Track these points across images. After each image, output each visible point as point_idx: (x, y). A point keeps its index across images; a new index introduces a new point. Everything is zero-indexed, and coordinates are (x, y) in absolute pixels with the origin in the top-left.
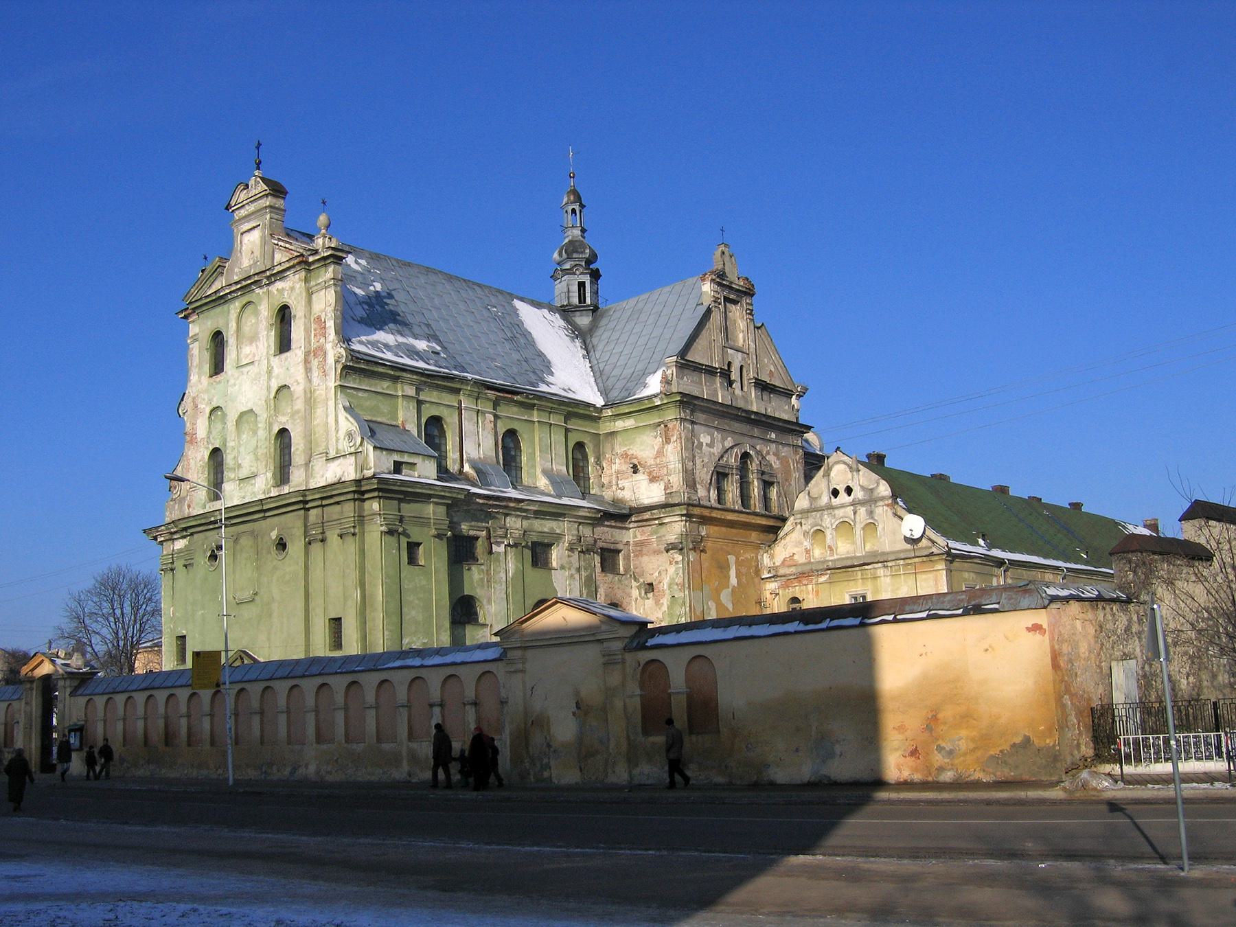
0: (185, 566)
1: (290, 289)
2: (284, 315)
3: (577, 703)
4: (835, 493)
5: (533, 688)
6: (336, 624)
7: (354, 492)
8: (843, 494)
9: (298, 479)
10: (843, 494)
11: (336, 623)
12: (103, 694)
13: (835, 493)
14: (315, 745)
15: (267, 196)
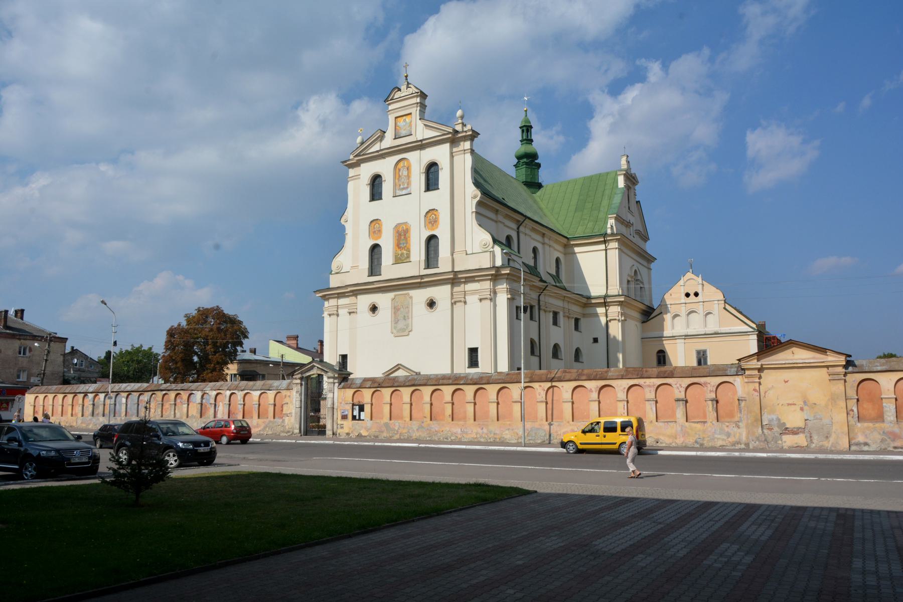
0: (350, 313)
1: (440, 154)
2: (432, 169)
3: (805, 402)
4: (688, 295)
5: (766, 392)
6: (473, 352)
7: (492, 275)
8: (692, 296)
9: (444, 265)
10: (692, 296)
11: (473, 352)
12: (370, 388)
13: (688, 295)
14: (571, 422)
15: (417, 96)
